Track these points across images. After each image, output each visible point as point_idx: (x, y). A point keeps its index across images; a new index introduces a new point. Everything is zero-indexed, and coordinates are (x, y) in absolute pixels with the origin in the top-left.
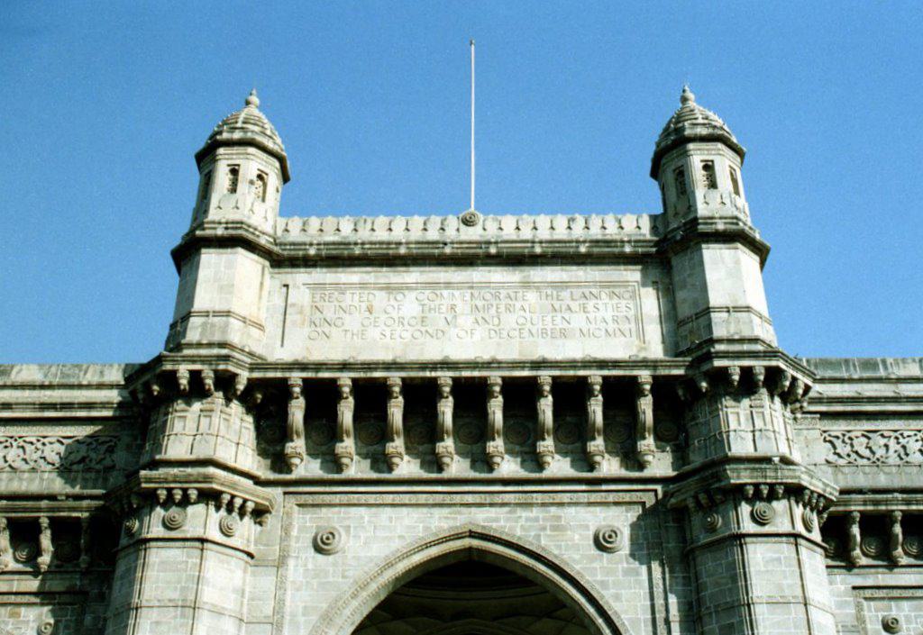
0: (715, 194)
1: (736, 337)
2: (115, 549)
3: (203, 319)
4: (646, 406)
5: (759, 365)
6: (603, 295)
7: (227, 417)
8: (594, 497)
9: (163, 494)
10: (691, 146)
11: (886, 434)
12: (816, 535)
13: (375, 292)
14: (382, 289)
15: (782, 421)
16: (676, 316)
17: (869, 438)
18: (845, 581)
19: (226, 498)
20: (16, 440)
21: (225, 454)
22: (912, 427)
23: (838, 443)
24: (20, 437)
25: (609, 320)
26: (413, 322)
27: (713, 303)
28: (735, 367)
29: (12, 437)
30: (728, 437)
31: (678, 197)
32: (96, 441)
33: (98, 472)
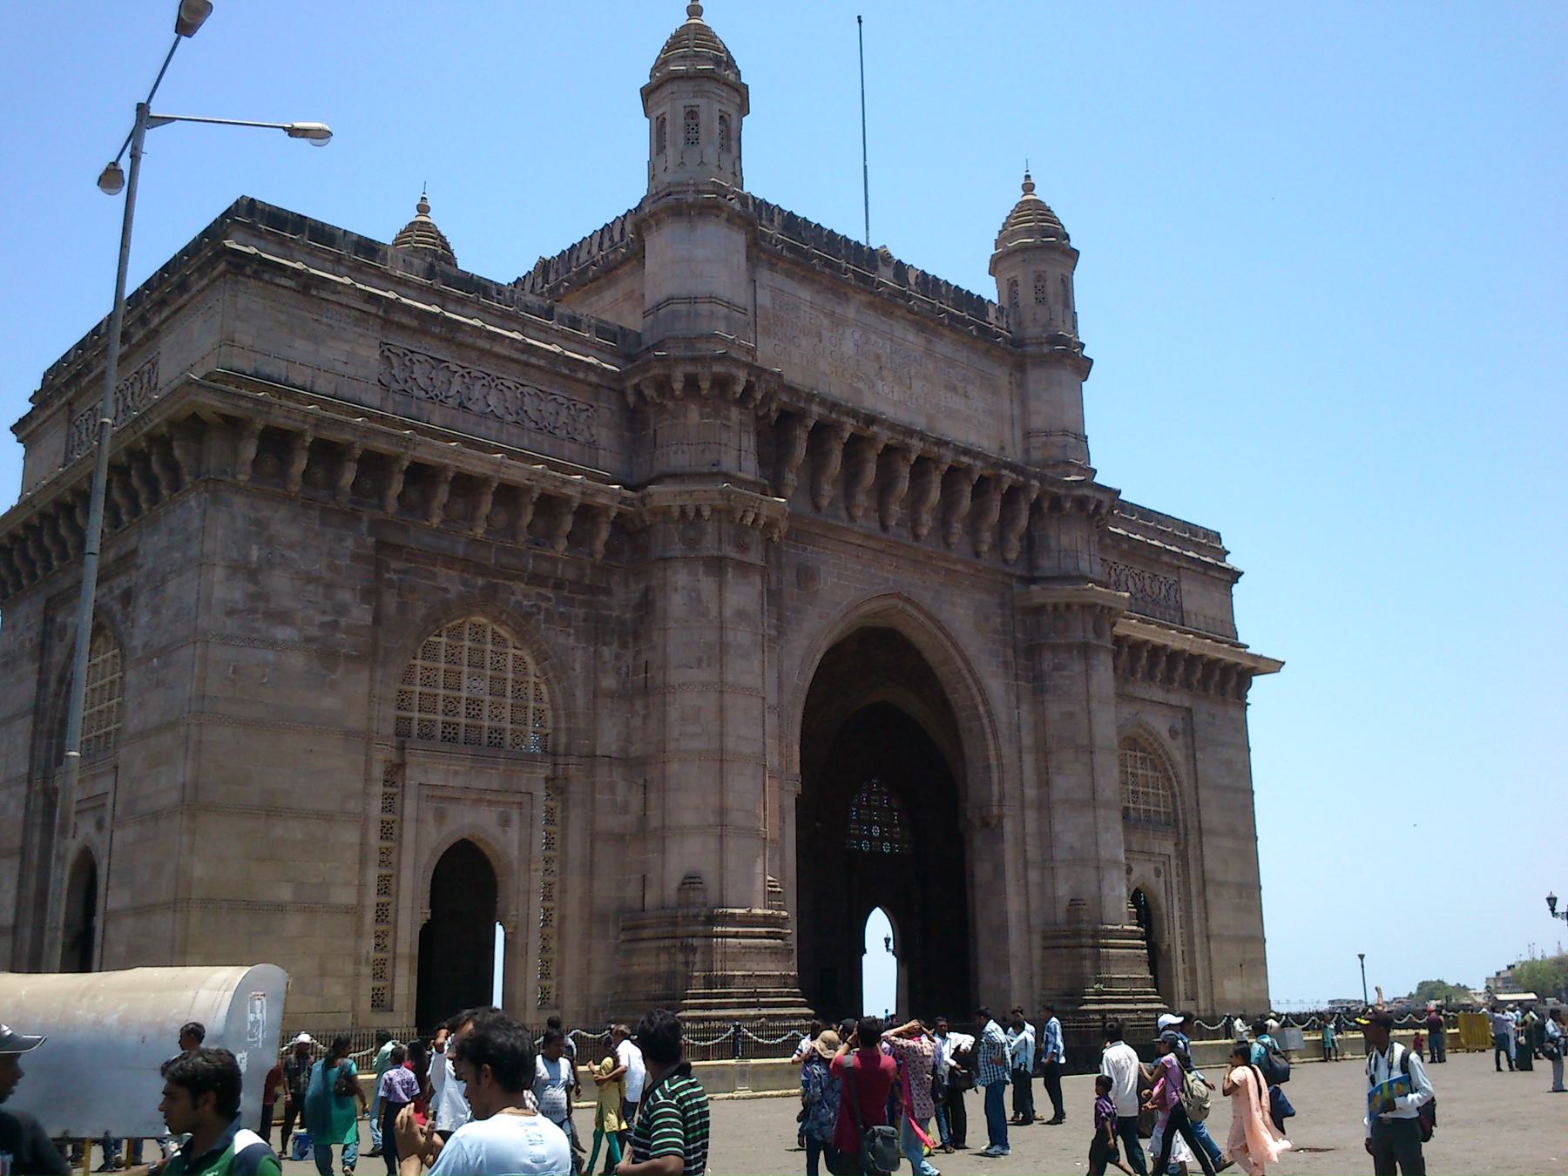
20: (493, 381)
24: (498, 378)
29: (489, 375)
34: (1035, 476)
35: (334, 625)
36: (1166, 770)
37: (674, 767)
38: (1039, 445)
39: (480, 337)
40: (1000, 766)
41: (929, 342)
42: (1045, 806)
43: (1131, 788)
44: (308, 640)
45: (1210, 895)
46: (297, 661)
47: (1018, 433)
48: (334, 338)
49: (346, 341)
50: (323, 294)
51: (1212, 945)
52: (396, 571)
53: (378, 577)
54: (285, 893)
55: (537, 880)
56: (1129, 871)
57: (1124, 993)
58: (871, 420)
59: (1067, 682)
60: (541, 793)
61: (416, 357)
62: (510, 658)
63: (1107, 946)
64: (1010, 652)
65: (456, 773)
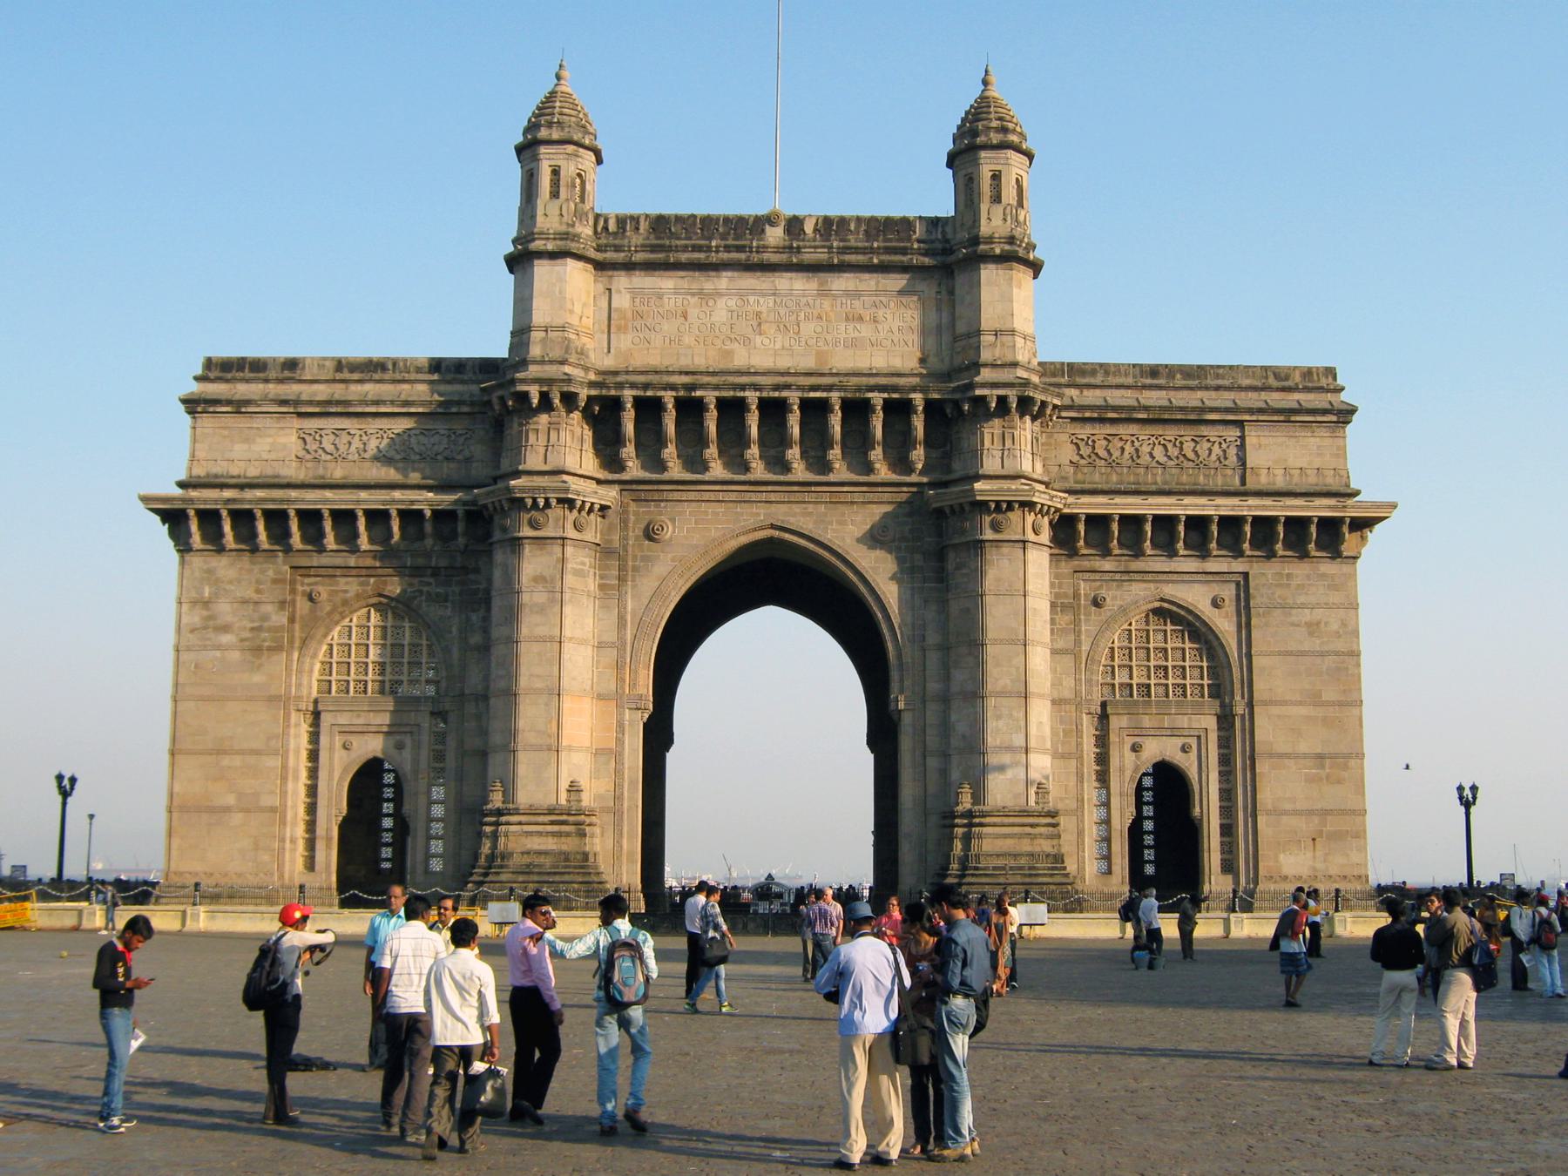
0: (998, 210)
1: (999, 363)
2: (491, 541)
3: (543, 334)
4: (918, 423)
5: (1012, 396)
6: (892, 304)
7: (572, 428)
8: (871, 497)
9: (529, 502)
10: (983, 154)
11: (1124, 437)
12: (1045, 536)
13: (689, 297)
14: (693, 295)
15: (1029, 437)
16: (954, 326)
17: (1109, 441)
18: (1066, 567)
19: (579, 503)
21: (571, 463)
22: (1147, 432)
23: (1082, 444)
25: (895, 330)
26: (724, 329)
27: (984, 326)
28: (992, 394)
30: (982, 454)
31: (966, 206)
32: (454, 433)
33: (459, 461)
34: (914, 389)
35: (259, 629)
36: (1207, 642)
37: (492, 701)
38: (959, 349)
39: (367, 405)
40: (901, 666)
41: (821, 284)
42: (945, 699)
43: (1152, 663)
44: (242, 640)
45: (1261, 767)
46: (235, 656)
47: (946, 338)
48: (261, 437)
49: (270, 436)
50: (250, 410)
51: (1262, 820)
52: (309, 585)
53: (293, 591)
54: (231, 800)
55: (423, 783)
56: (1135, 748)
57: (995, 868)
58: (692, 387)
59: (966, 580)
60: (426, 722)
61: (323, 433)
62: (407, 628)
63: (981, 825)
64: (918, 557)
65: (359, 716)
